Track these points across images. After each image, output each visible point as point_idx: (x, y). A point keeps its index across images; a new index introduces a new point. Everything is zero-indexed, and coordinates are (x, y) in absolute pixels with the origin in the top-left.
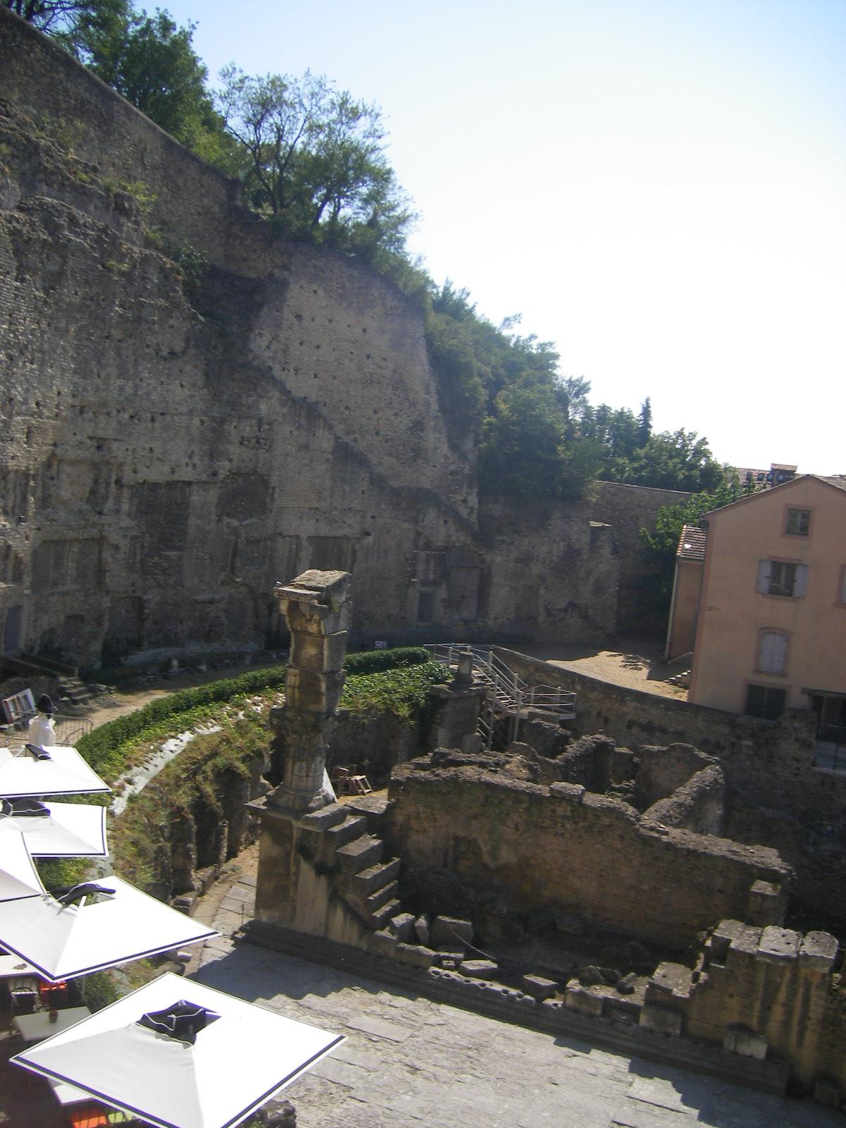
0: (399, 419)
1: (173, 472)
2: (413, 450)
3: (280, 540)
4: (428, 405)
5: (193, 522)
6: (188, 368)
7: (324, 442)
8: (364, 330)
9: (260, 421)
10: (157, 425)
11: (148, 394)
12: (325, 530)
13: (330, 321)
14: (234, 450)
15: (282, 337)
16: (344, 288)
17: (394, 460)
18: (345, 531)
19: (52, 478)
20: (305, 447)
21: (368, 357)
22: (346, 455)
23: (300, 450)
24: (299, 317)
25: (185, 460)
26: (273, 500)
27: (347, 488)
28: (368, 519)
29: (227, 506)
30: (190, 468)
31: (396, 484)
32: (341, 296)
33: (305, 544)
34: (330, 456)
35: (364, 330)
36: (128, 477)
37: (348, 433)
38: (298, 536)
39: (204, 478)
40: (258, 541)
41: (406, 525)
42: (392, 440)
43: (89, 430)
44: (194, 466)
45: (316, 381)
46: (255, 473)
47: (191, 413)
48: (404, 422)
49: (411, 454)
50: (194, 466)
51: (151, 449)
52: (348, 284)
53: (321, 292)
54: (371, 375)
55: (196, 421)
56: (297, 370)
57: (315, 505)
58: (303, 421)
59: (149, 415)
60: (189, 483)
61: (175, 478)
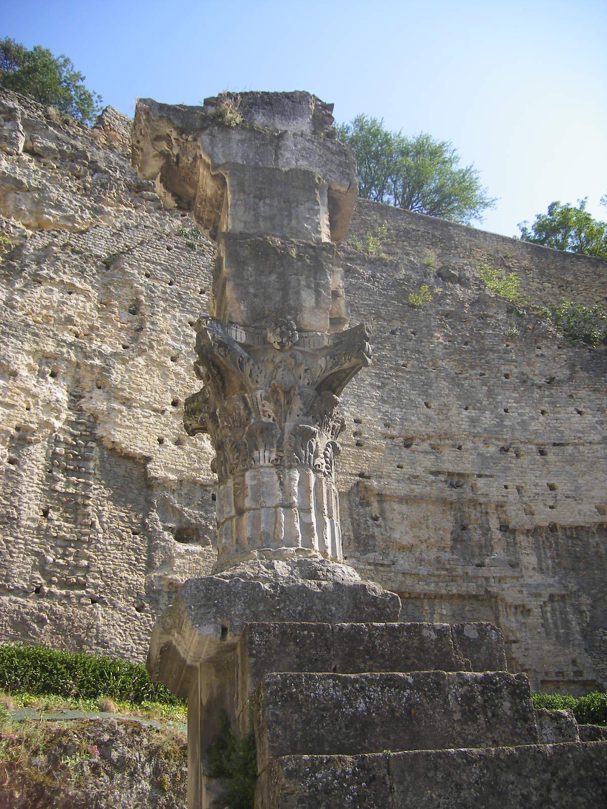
6: (583, 393)
10: (551, 457)
11: (523, 424)
19: (375, 519)
36: (516, 516)
43: (428, 461)
51: (552, 487)
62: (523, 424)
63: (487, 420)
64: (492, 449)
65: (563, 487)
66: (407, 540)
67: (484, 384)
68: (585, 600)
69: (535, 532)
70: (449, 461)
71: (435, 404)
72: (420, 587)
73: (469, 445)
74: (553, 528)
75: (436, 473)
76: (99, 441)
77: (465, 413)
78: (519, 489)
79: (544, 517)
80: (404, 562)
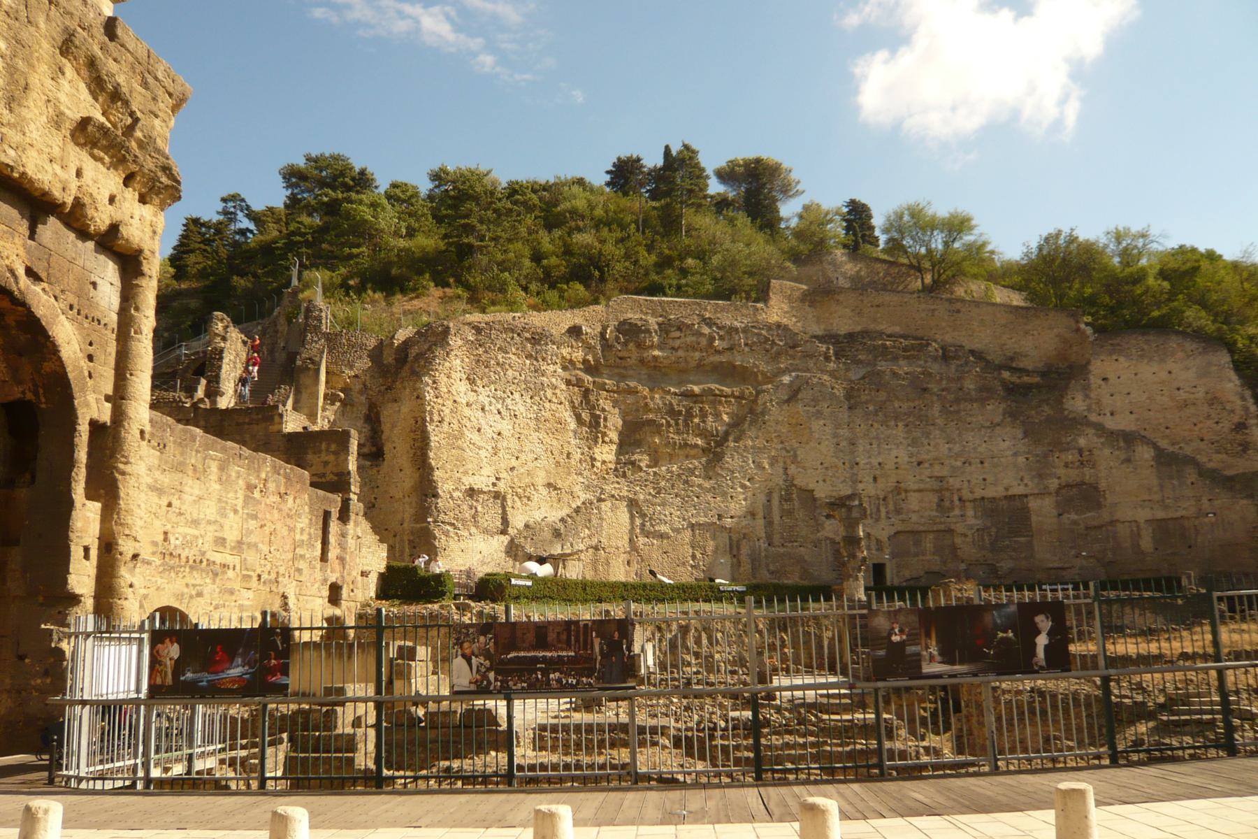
0: (1221, 425)
1: (1007, 489)
2: (1240, 445)
3: (1120, 527)
4: (1246, 409)
5: (1034, 518)
7: (1145, 454)
8: (1170, 372)
9: (1081, 451)
10: (986, 465)
11: (975, 449)
12: (1160, 514)
13: (1136, 374)
14: (1061, 471)
15: (1092, 395)
16: (1143, 350)
17: (1224, 456)
18: (1183, 513)
20: (1128, 460)
21: (1178, 389)
22: (1168, 461)
23: (1122, 463)
24: (1105, 379)
25: (1015, 483)
26: (1105, 499)
27: (1175, 482)
28: (1205, 500)
29: (1064, 506)
30: (1022, 487)
31: (1228, 473)
32: (1141, 356)
33: (1142, 525)
34: (1153, 463)
35: (1170, 372)
36: (966, 495)
37: (1173, 444)
38: (1136, 521)
39: (1036, 491)
40: (1099, 527)
41: (1245, 502)
42: (1217, 442)
43: (928, 472)
44: (1026, 485)
45: (1133, 416)
46: (1083, 483)
47: (1015, 454)
48: (1226, 425)
49: (1240, 448)
50: (1026, 485)
51: (984, 480)
52: (1146, 347)
53: (1122, 359)
54: (1185, 401)
55: (1021, 459)
56: (1112, 414)
57: (1147, 497)
58: (1122, 444)
59: (978, 461)
60: (1026, 496)
61: (1010, 493)
62: (975, 449)
63: (957, 448)
64: (959, 464)
65: (990, 479)
66: (917, 508)
67: (958, 429)
68: (994, 530)
69: (975, 500)
70: (937, 471)
71: (932, 443)
72: (921, 528)
73: (947, 462)
74: (983, 498)
75: (931, 477)
76: (795, 486)
77: (947, 446)
78: (969, 481)
79: (979, 493)
80: (914, 518)
